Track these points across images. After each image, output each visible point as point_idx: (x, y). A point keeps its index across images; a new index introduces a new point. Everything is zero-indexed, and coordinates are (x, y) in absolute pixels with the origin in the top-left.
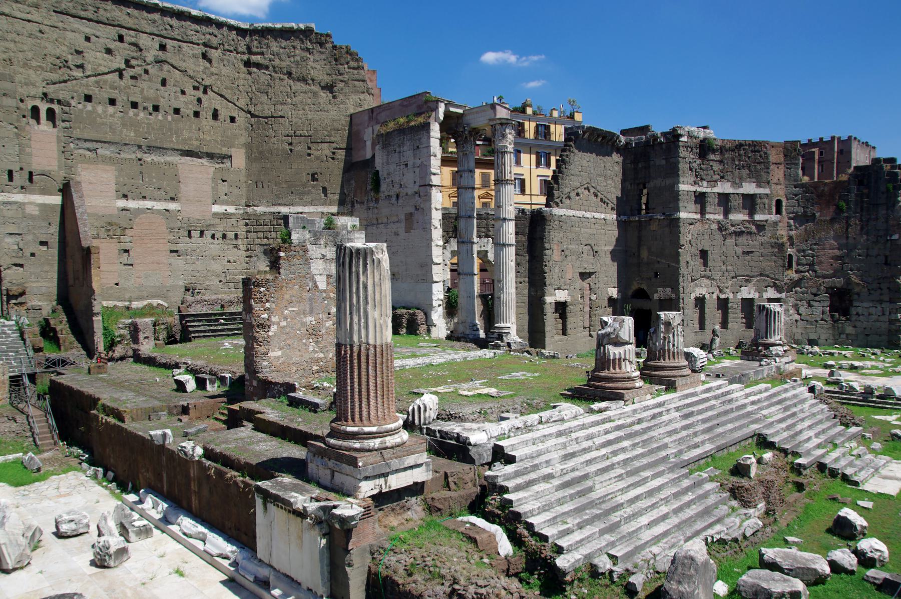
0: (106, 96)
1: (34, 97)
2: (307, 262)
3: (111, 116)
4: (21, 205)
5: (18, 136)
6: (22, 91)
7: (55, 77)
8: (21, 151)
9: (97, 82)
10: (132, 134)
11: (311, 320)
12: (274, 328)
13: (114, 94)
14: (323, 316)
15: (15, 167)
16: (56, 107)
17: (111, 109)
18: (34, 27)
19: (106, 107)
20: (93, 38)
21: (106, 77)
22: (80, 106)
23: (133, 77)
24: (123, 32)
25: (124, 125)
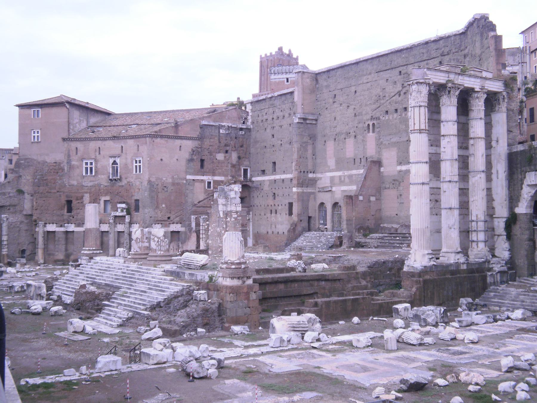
0: (393, 108)
1: (368, 120)
2: (218, 205)
3: (396, 119)
4: (362, 174)
5: (363, 140)
6: (365, 118)
7: (374, 106)
8: (364, 148)
9: (390, 103)
10: (404, 127)
11: (218, 229)
12: (210, 231)
13: (397, 106)
14: (221, 228)
15: (362, 157)
16: (375, 122)
17: (395, 115)
18: (369, 85)
19: (393, 115)
20: (389, 79)
21: (394, 98)
22: (384, 118)
23: (405, 93)
24: (400, 69)
25: (400, 123)
